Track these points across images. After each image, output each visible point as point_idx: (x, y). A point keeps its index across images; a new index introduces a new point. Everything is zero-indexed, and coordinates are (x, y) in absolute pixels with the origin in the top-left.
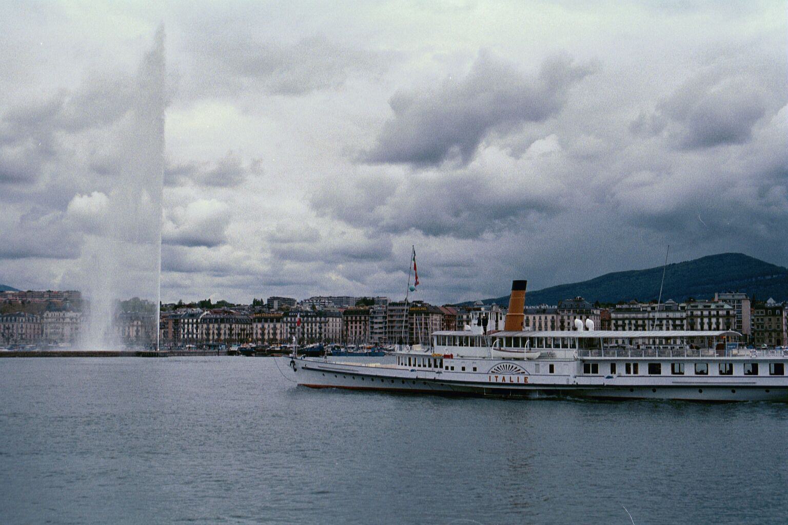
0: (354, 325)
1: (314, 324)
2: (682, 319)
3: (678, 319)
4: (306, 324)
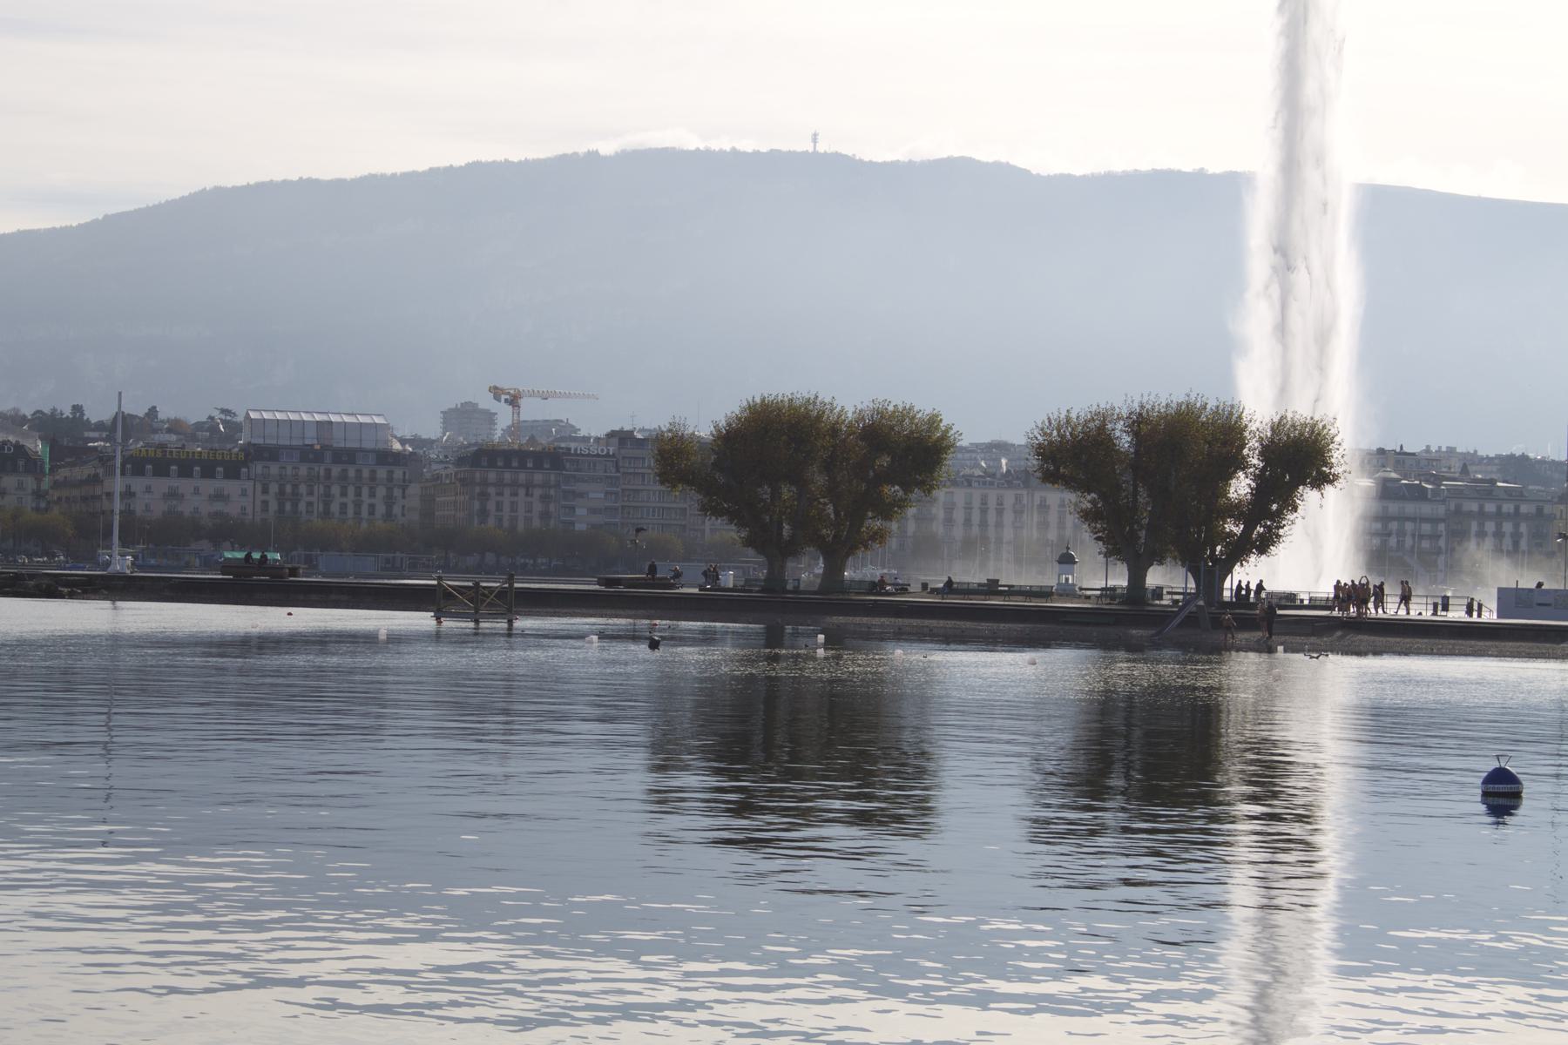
0: (507, 499)
1: (365, 491)
2: (1434, 521)
3: (1424, 520)
4: (335, 490)
